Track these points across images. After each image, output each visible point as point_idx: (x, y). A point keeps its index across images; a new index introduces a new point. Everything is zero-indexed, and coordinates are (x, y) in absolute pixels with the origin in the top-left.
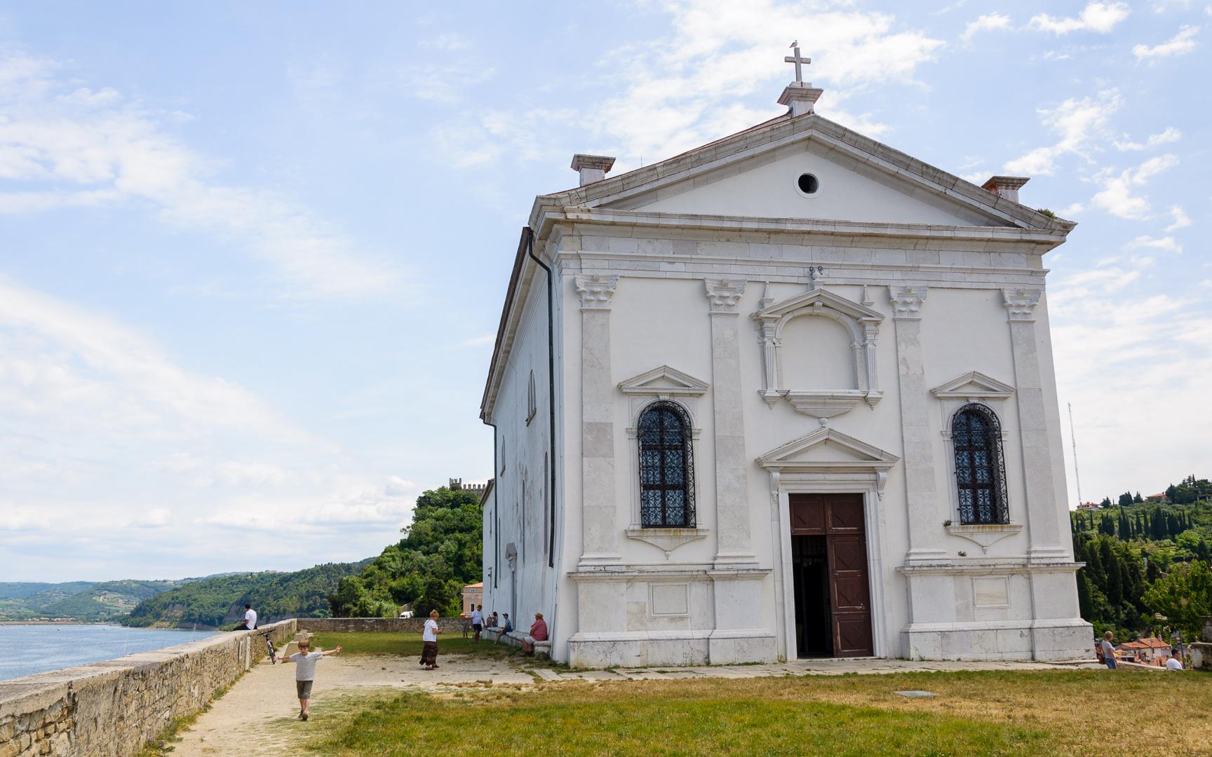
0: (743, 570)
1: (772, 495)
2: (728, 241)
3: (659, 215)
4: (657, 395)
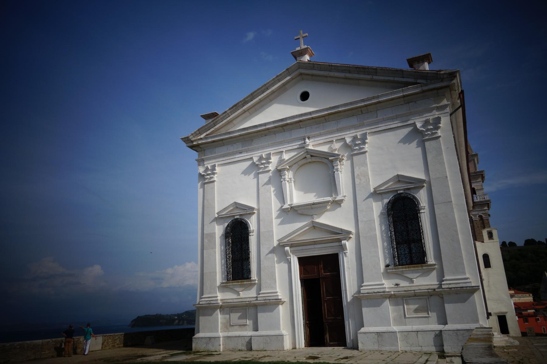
2: (266, 135)
3: (230, 133)
4: (234, 216)
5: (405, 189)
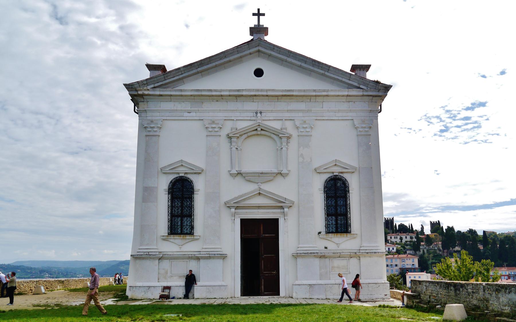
0: (212, 254)
1: (232, 219)
2: (217, 101)
3: (181, 90)
5: (339, 172)
